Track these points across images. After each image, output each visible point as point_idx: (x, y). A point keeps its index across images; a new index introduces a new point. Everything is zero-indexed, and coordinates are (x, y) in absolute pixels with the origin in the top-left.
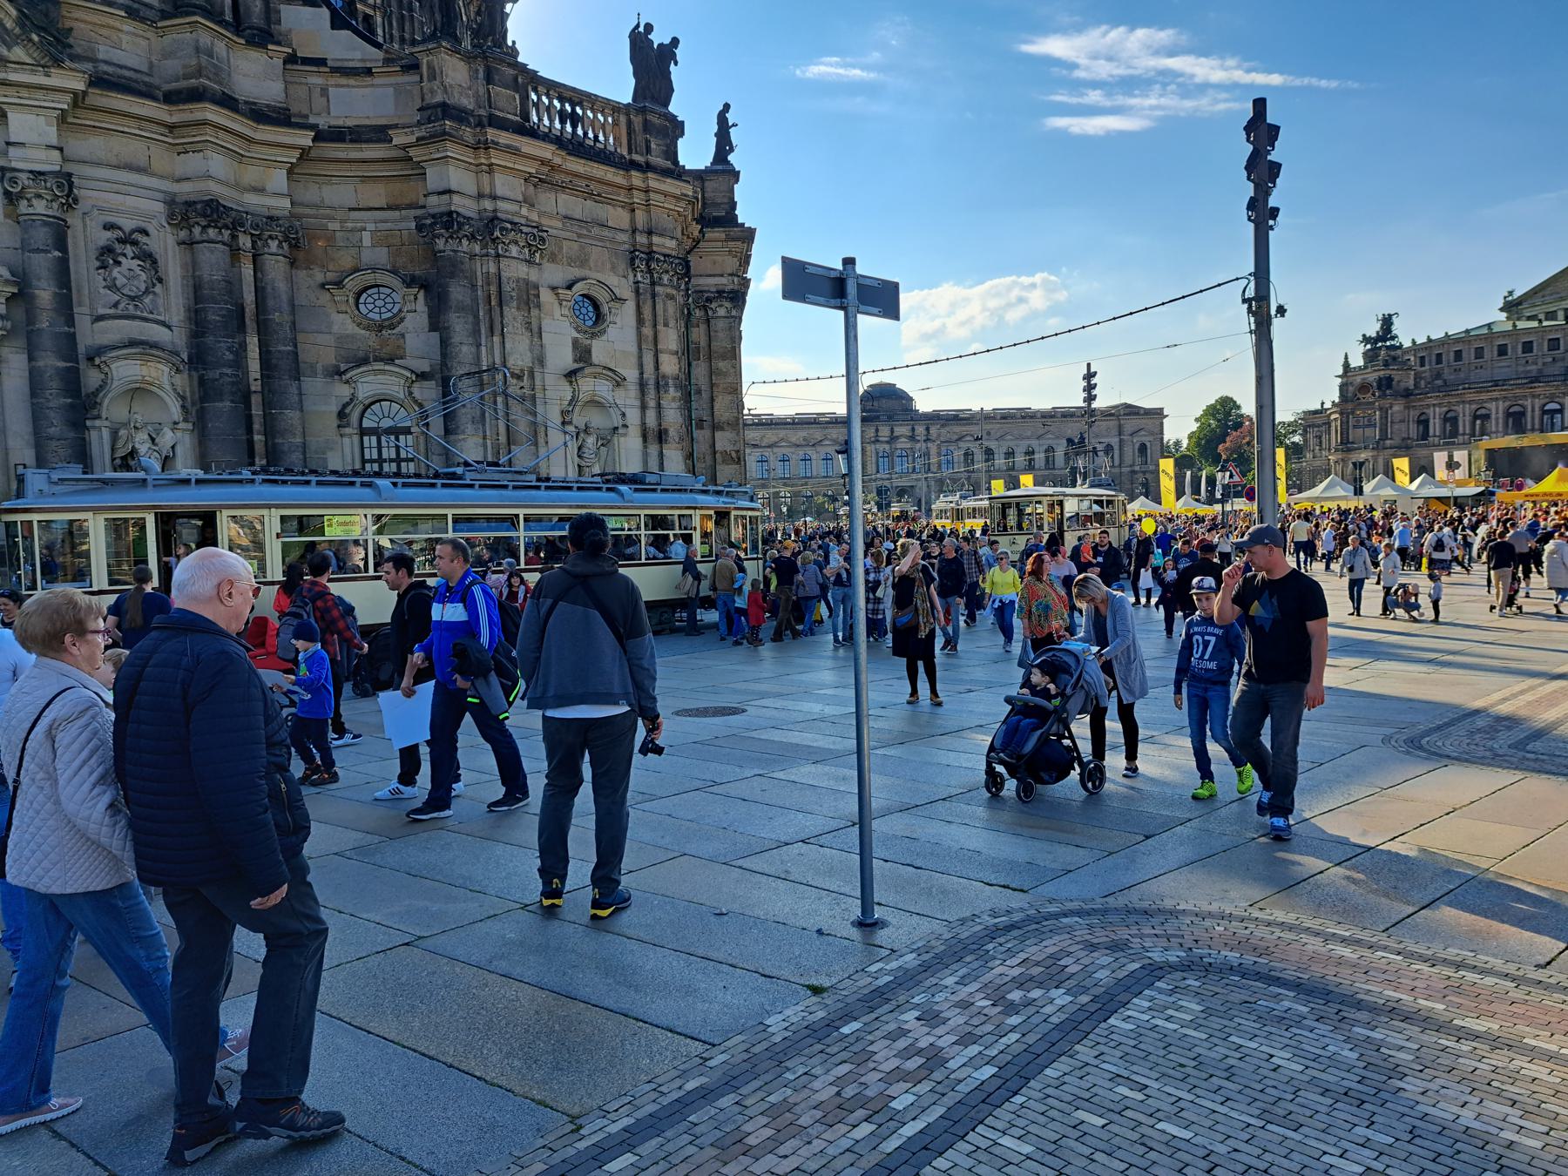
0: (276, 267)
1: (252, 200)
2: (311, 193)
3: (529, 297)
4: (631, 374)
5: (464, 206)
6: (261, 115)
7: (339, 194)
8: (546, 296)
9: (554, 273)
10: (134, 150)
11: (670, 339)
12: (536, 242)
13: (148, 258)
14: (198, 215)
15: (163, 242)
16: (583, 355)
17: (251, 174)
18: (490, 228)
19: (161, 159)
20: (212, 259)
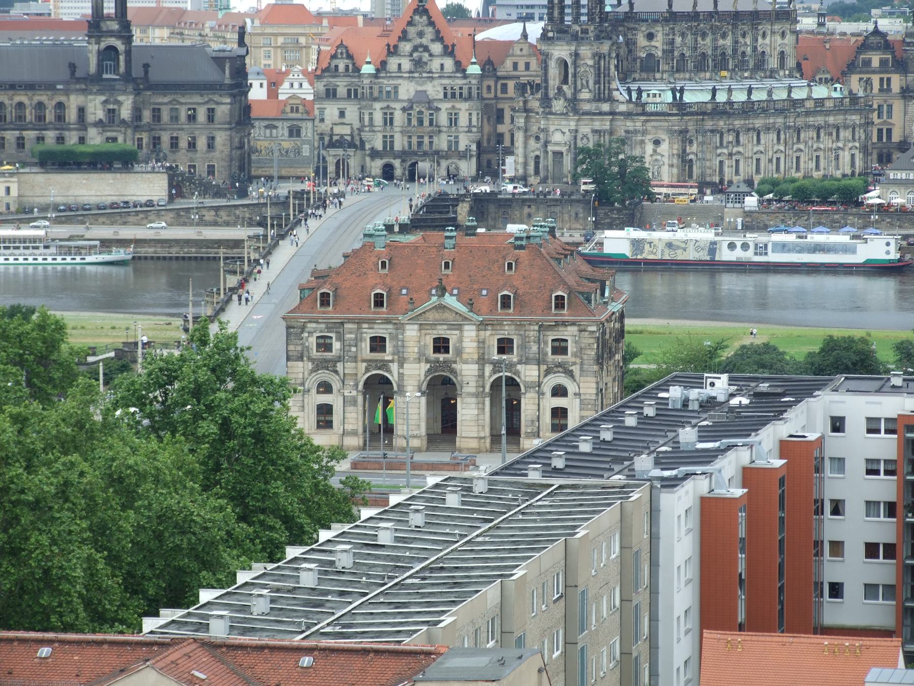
0: (607, 137)
1: (605, 127)
2: (614, 123)
3: (642, 142)
4: (666, 154)
5: (631, 129)
6: (606, 114)
7: (619, 123)
8: (646, 141)
9: (649, 137)
10: (587, 122)
11: (676, 146)
12: (644, 133)
13: (588, 139)
14: (595, 131)
15: (590, 136)
16: (655, 151)
17: (604, 123)
18: (636, 132)
19: (590, 123)
20: (596, 137)
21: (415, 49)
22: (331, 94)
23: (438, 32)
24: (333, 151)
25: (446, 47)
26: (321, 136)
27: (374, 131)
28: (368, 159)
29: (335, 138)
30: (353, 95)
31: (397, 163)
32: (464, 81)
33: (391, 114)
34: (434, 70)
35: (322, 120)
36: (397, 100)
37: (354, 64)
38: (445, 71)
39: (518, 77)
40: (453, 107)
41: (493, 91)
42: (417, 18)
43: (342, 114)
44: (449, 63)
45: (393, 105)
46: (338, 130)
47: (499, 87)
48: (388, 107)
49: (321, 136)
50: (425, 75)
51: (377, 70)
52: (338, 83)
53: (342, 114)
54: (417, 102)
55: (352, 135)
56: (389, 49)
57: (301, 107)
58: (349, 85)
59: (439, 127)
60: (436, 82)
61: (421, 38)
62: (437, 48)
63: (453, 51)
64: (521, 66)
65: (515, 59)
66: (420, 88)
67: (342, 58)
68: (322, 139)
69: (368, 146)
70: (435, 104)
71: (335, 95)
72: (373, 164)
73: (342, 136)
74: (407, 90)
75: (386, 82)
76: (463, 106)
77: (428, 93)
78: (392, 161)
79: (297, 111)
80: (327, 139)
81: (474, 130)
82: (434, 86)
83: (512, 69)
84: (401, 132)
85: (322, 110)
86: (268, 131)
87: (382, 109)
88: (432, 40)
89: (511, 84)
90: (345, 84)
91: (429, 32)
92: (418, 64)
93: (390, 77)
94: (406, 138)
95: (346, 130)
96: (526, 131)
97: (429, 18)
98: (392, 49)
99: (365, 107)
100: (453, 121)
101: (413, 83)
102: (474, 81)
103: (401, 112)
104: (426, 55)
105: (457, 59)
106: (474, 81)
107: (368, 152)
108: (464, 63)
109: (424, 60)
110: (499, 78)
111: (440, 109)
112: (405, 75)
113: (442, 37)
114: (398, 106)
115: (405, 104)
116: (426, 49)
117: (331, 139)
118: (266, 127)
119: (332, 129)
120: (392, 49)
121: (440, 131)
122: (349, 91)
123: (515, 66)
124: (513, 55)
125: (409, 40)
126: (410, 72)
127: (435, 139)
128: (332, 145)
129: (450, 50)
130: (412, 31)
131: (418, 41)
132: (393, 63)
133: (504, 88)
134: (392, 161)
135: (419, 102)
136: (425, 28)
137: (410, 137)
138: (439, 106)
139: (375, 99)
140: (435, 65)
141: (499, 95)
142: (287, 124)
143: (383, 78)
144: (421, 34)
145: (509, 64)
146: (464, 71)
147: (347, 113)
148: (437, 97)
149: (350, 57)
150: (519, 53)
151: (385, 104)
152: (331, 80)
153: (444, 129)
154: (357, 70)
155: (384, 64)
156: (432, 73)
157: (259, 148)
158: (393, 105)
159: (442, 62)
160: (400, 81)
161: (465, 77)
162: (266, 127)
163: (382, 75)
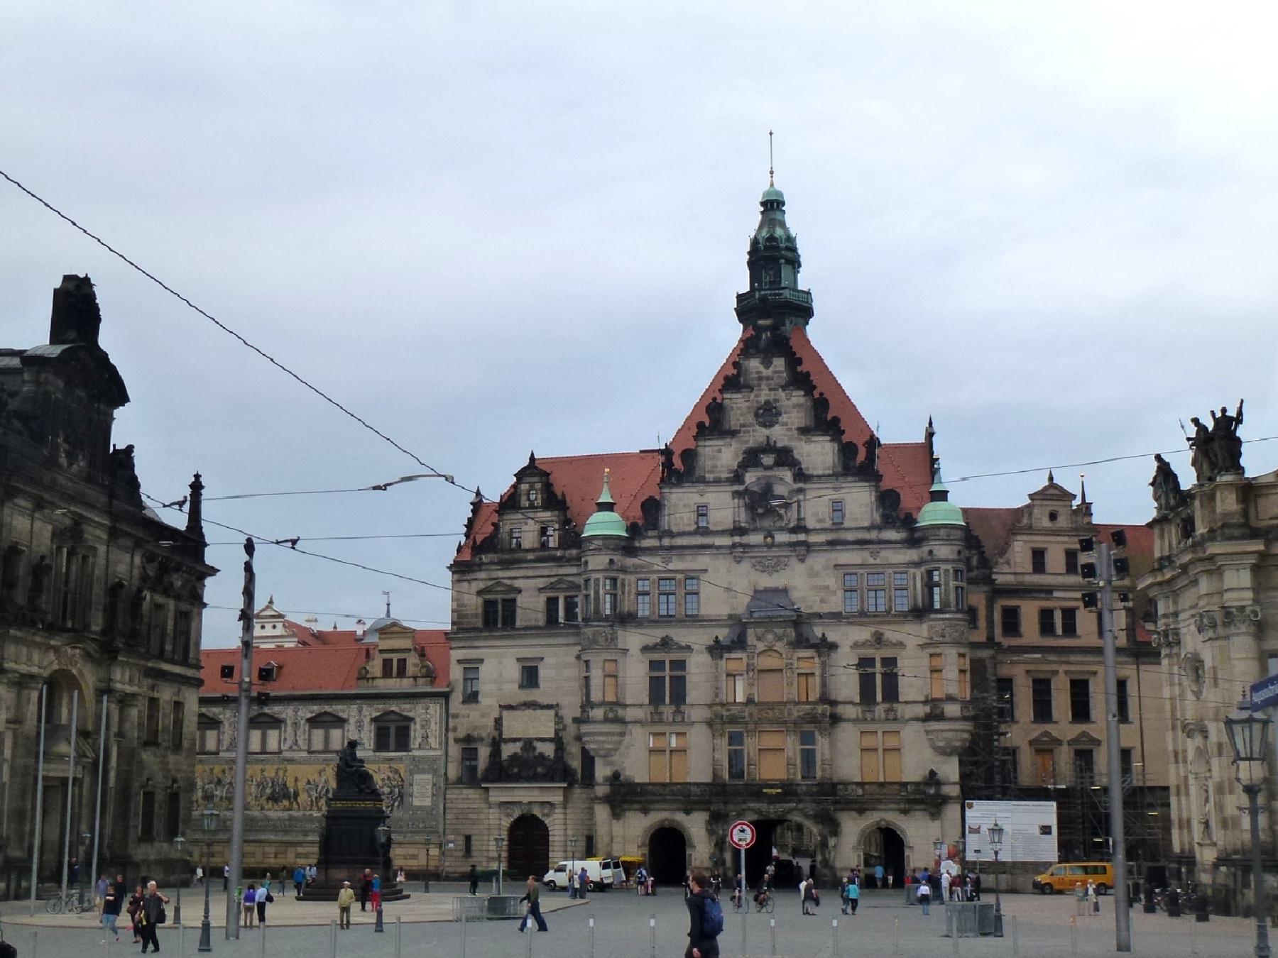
21: (751, 458)
22: (496, 617)
23: (820, 405)
24: (498, 794)
25: (847, 450)
26: (469, 744)
27: (622, 721)
28: (602, 812)
29: (508, 750)
30: (561, 617)
31: (695, 826)
32: (912, 555)
33: (680, 665)
34: (811, 523)
35: (472, 698)
36: (694, 620)
37: (567, 521)
38: (847, 524)
39: (1048, 591)
40: (879, 639)
41: (982, 623)
42: (754, 364)
43: (530, 676)
44: (859, 501)
45: (681, 635)
46: (517, 726)
47: (997, 617)
48: (666, 643)
49: (469, 744)
50: (782, 538)
51: (634, 530)
52: (518, 583)
53: (530, 676)
54: (757, 624)
55: (558, 741)
56: (668, 464)
57: (412, 661)
58: (551, 587)
59: (834, 703)
60: (819, 561)
61: (769, 425)
62: (819, 454)
63: (871, 458)
64: (1055, 559)
65: (1039, 541)
66: (766, 581)
67: (532, 506)
68: (469, 754)
69: (602, 771)
70: (818, 631)
71: (509, 620)
72: (618, 828)
73: (528, 744)
74: (725, 586)
75: (656, 562)
76: (911, 635)
77: (794, 595)
78: (680, 817)
79: (402, 673)
80: (484, 752)
81: (952, 709)
82: (813, 574)
83: (1029, 568)
84: (710, 724)
85: (471, 668)
86: (318, 734)
87: (645, 649)
88: (804, 431)
89: (1029, 611)
90: (541, 583)
91: (794, 408)
92: (760, 504)
93: (671, 548)
94: (723, 743)
95: (539, 726)
96: (1260, 629)
97: (794, 362)
98: (677, 463)
99: (590, 645)
100: (879, 683)
101: (746, 566)
102: (944, 551)
103: (705, 658)
104: (787, 475)
105: (886, 484)
106: (944, 551)
107: (601, 790)
108: (907, 501)
109: (779, 489)
110: (999, 592)
111: (833, 647)
112: (719, 541)
113: (836, 420)
114: (698, 638)
115: (723, 634)
116: (785, 457)
117: (496, 753)
118: (314, 722)
119: (498, 722)
120: (677, 463)
121: (835, 719)
122: (552, 603)
123: (1038, 558)
124: (1030, 530)
125: (733, 434)
126: (738, 530)
127: (821, 745)
128: (501, 772)
129: (861, 456)
130: (739, 406)
131: (758, 435)
132: (681, 505)
133: (1011, 622)
134: (680, 817)
135: (768, 623)
136: (782, 394)
137: (735, 739)
138: (831, 637)
139: (626, 619)
140: (815, 507)
141: (998, 637)
142: (371, 711)
143: (651, 551)
144: (768, 414)
145: (1020, 551)
146: (908, 522)
147: (543, 673)
148: (825, 609)
149: (553, 501)
150: (1046, 523)
151: (657, 634)
152: (501, 574)
153: (850, 712)
154: (572, 538)
155: (652, 508)
156: (805, 530)
157: (291, 784)
158: (681, 635)
159: (836, 496)
160: (703, 561)
161: (916, 537)
162: (314, 722)
163: (647, 543)
